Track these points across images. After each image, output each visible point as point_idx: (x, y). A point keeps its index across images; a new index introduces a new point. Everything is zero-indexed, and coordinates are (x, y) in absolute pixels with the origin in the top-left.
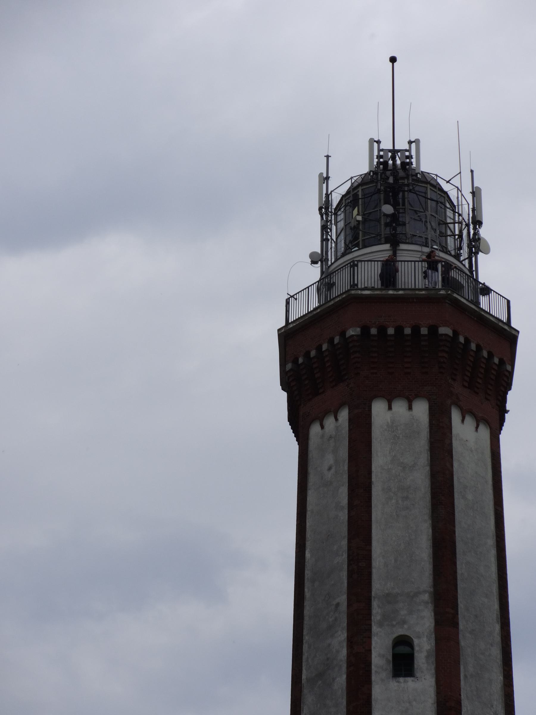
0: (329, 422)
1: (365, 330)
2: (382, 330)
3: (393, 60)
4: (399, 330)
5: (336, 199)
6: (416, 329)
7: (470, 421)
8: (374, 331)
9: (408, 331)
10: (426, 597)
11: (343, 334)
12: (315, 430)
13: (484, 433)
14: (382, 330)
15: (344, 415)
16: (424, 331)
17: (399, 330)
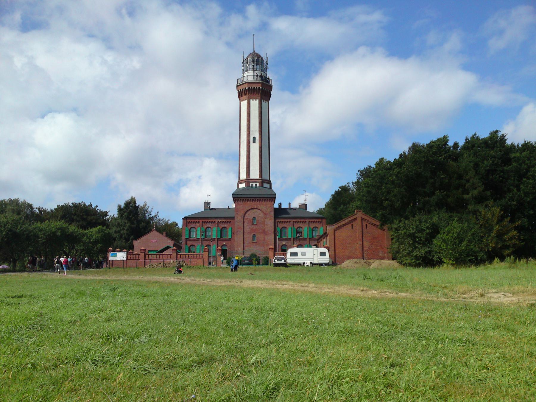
0: (244, 101)
1: (249, 88)
2: (252, 88)
3: (254, 35)
4: (254, 88)
5: (245, 59)
6: (257, 88)
7: (265, 101)
8: (250, 88)
9: (255, 88)
10: (258, 131)
11: (246, 88)
12: (242, 102)
13: (267, 102)
14: (252, 88)
15: (246, 101)
16: (258, 88)
17: (254, 88)
